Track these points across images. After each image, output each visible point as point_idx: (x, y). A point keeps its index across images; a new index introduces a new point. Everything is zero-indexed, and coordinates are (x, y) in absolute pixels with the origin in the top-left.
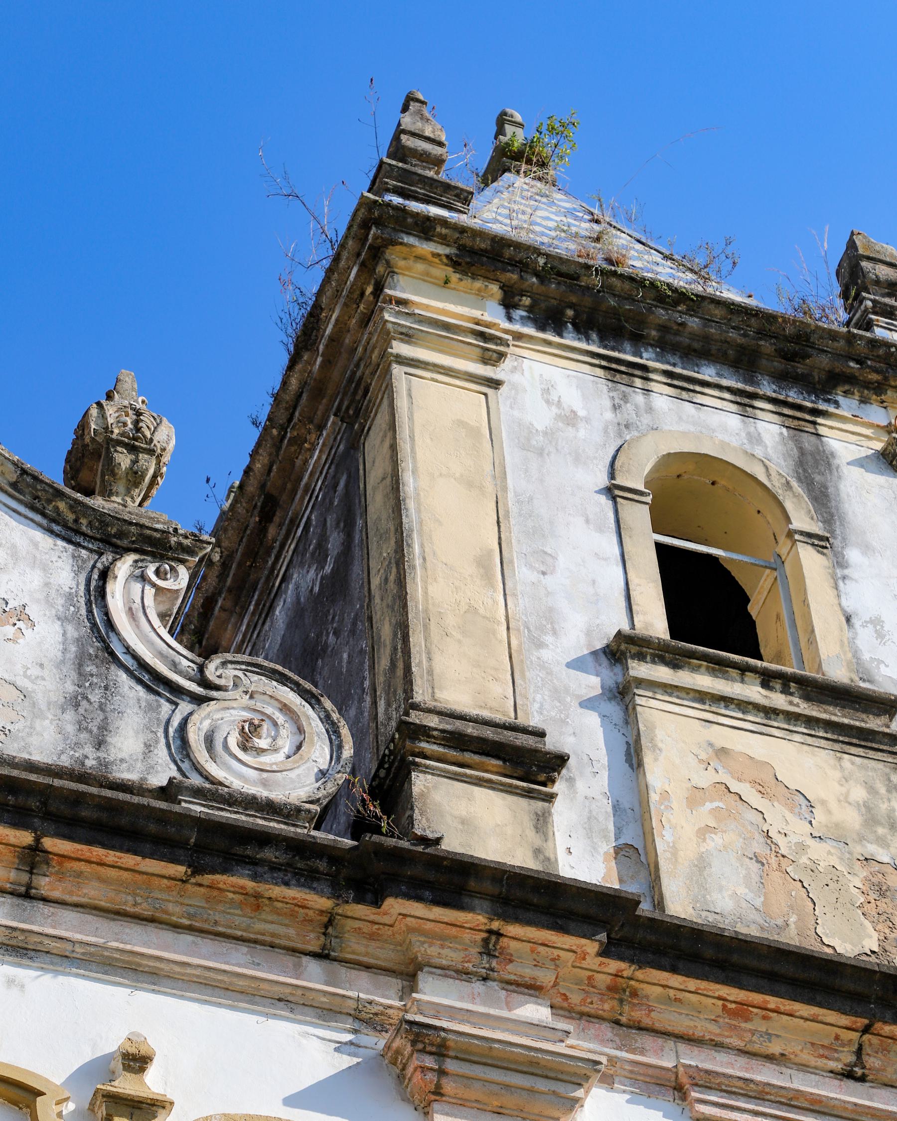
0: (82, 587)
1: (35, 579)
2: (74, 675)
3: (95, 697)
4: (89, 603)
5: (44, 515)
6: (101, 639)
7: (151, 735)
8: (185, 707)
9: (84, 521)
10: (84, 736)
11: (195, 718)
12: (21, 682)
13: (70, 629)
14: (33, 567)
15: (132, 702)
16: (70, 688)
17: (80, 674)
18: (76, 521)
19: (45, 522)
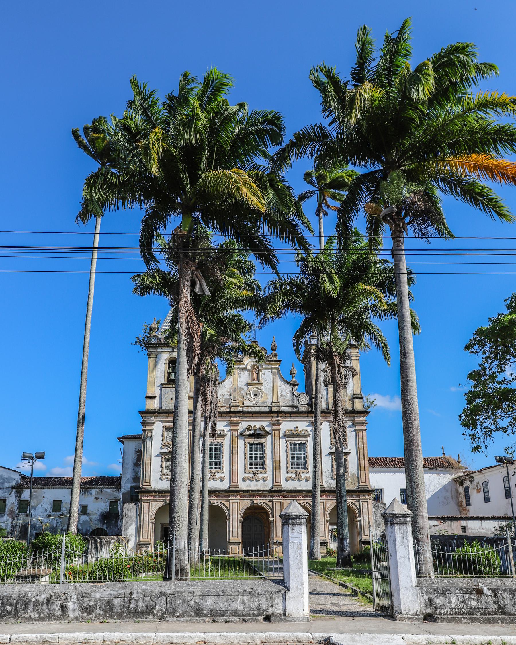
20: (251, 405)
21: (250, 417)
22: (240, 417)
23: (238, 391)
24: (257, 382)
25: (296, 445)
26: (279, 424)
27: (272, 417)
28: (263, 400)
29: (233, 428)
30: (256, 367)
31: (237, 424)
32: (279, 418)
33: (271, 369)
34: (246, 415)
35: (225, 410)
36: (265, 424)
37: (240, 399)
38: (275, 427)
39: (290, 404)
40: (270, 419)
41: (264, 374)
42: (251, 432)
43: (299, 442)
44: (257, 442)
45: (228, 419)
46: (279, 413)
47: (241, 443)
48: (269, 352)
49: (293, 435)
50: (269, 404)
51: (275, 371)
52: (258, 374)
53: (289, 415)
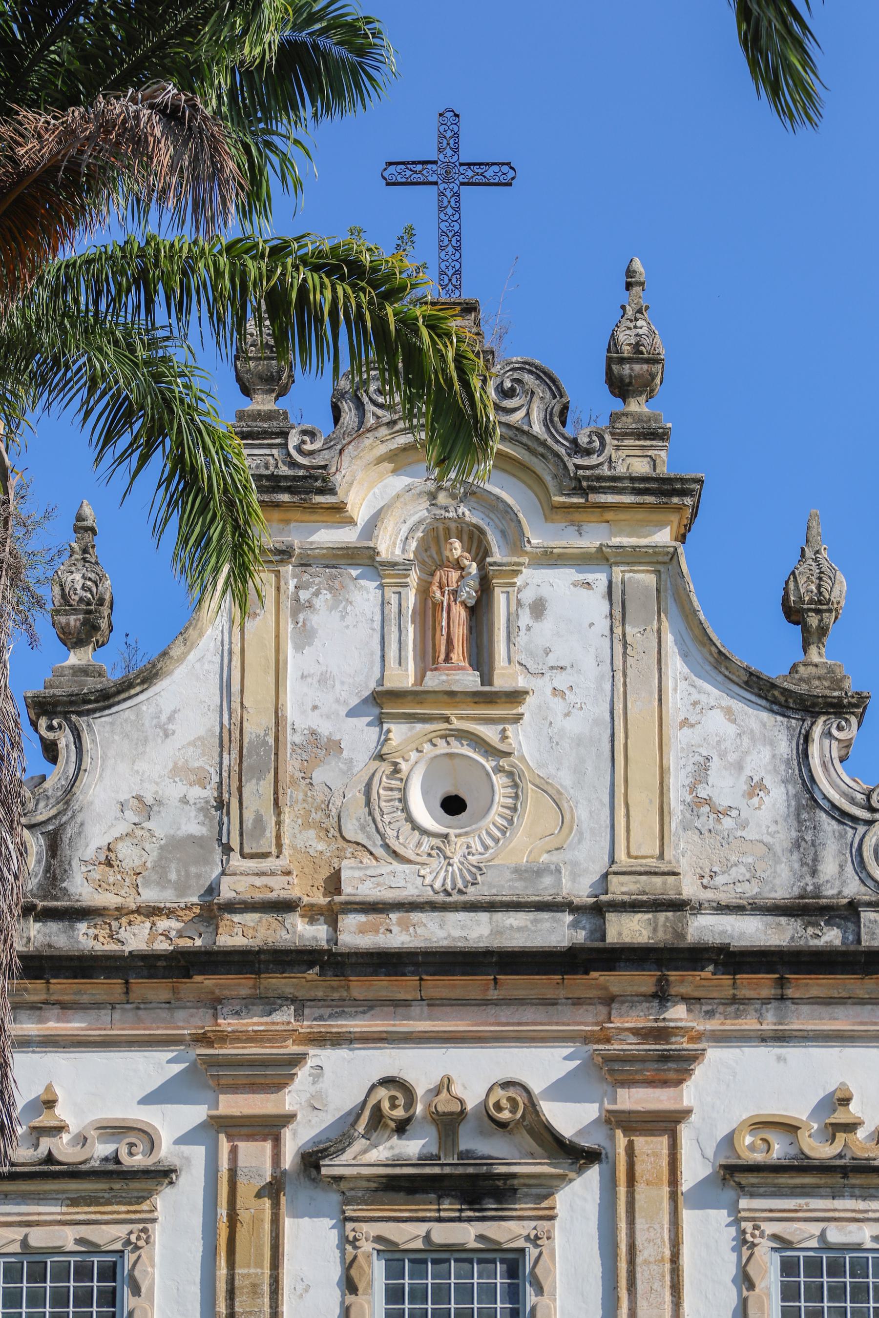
0: (794, 752)
1: (766, 754)
2: (795, 824)
3: (808, 838)
4: (799, 764)
5: (767, 700)
6: (809, 792)
7: (843, 857)
8: (861, 829)
9: (791, 701)
10: (805, 868)
11: (867, 838)
12: (767, 839)
13: (790, 787)
14: (764, 745)
15: (830, 834)
16: (794, 834)
17: (799, 822)
18: (786, 701)
19: (767, 705)
20: (412, 891)
21: (399, 1004)
22: (300, 1004)
23: (291, 765)
24: (470, 680)
25: (836, 1269)
26: (673, 1066)
27: (609, 1000)
28: (523, 846)
29: (233, 1105)
30: (457, 548)
31: (275, 1073)
32: (678, 1013)
33: (602, 558)
34: (360, 987)
35: (162, 946)
36: (542, 1066)
37: (302, 839)
38: (636, 1099)
39: (782, 885)
40: (585, 1021)
41: (538, 608)
42: (412, 1147)
43: (864, 1234)
44: (466, 1234)
45: (189, 1022)
46: (671, 961)
47: (311, 1244)
48: (591, 403)
49: (799, 1174)
50: (581, 890)
51: (644, 579)
52: (479, 612)
53: (761, 984)
